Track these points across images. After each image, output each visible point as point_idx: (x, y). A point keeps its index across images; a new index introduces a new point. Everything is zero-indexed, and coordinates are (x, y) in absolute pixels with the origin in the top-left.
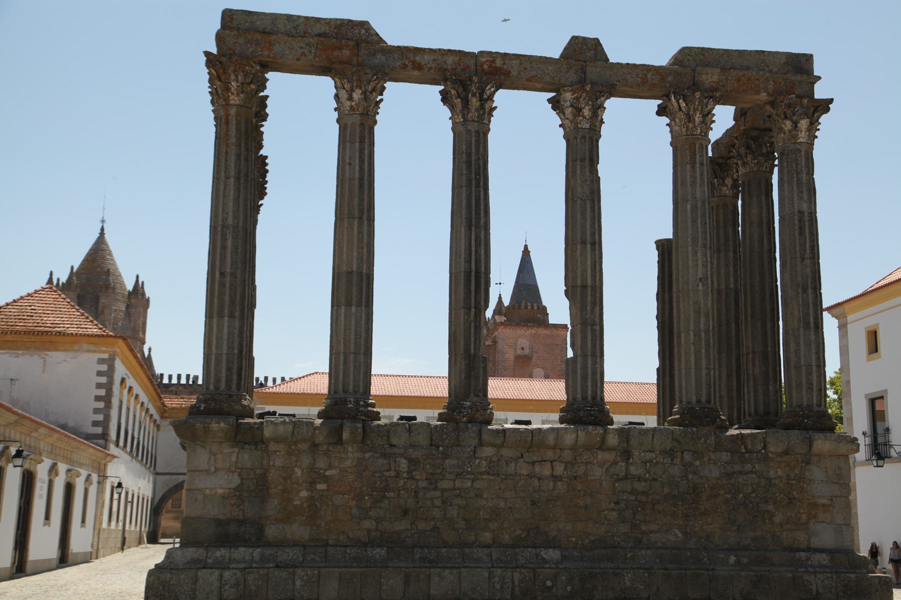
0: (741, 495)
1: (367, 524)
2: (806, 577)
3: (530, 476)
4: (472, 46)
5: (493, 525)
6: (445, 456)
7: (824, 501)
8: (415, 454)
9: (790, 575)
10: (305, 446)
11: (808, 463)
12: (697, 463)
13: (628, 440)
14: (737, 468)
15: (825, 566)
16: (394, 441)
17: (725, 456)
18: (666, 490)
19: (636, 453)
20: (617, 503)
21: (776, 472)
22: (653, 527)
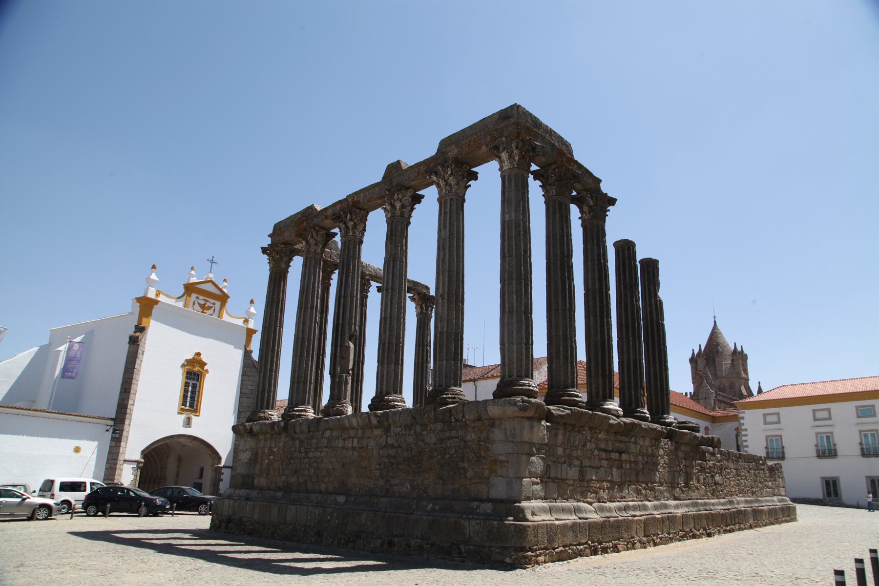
0: (447, 456)
1: (284, 478)
2: (463, 522)
3: (343, 448)
4: (343, 197)
5: (326, 480)
6: (312, 438)
7: (502, 458)
8: (302, 437)
9: (453, 520)
10: (268, 436)
11: (493, 426)
12: (424, 433)
13: (387, 419)
14: (447, 434)
15: (487, 514)
16: (298, 430)
17: (439, 426)
18: (405, 454)
19: (392, 428)
20: (380, 465)
21: (471, 436)
22: (396, 481)
